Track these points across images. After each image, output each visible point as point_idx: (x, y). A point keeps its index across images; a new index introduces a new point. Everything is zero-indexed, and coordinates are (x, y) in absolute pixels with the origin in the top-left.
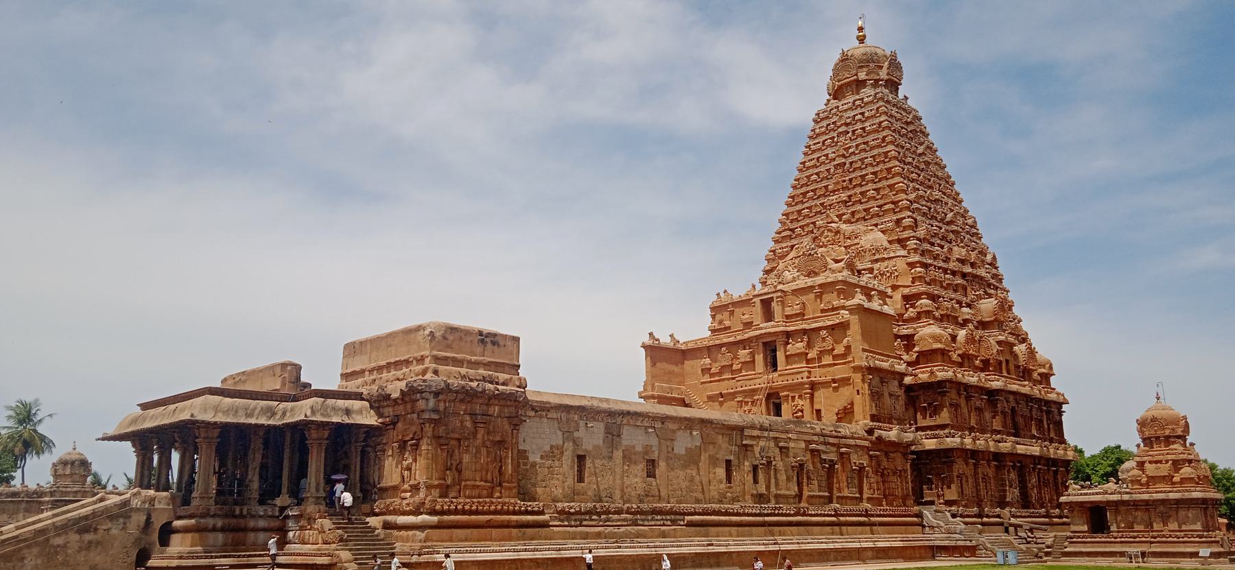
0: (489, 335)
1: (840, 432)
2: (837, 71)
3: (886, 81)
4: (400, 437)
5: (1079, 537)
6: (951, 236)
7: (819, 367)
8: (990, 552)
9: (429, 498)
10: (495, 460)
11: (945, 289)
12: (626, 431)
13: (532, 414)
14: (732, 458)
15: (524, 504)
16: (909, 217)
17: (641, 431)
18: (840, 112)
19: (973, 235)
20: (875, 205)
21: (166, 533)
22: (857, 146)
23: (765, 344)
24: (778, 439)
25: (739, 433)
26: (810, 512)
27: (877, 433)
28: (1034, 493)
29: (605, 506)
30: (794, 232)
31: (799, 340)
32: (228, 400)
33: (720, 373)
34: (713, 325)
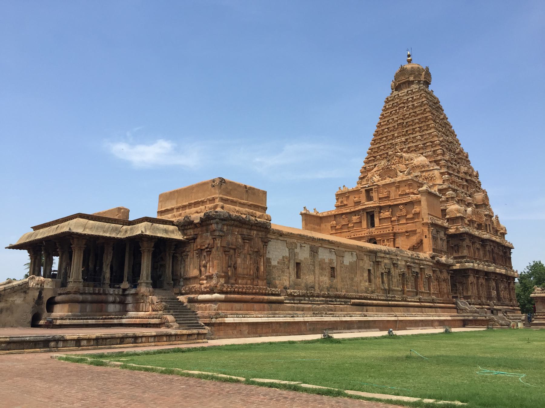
0: (251, 188)
1: (419, 257)
2: (397, 77)
3: (424, 81)
5: (541, 315)
6: (459, 161)
7: (398, 225)
8: (497, 323)
9: (219, 284)
10: (255, 263)
11: (459, 187)
12: (320, 250)
13: (273, 237)
14: (371, 268)
15: (270, 290)
16: (440, 149)
17: (328, 251)
18: (400, 97)
20: (421, 143)
21: (51, 304)
22: (410, 114)
23: (367, 213)
24: (393, 259)
25: (374, 255)
27: (436, 259)
28: (502, 293)
29: (312, 292)
32: (91, 222)
33: (341, 228)
34: (337, 203)
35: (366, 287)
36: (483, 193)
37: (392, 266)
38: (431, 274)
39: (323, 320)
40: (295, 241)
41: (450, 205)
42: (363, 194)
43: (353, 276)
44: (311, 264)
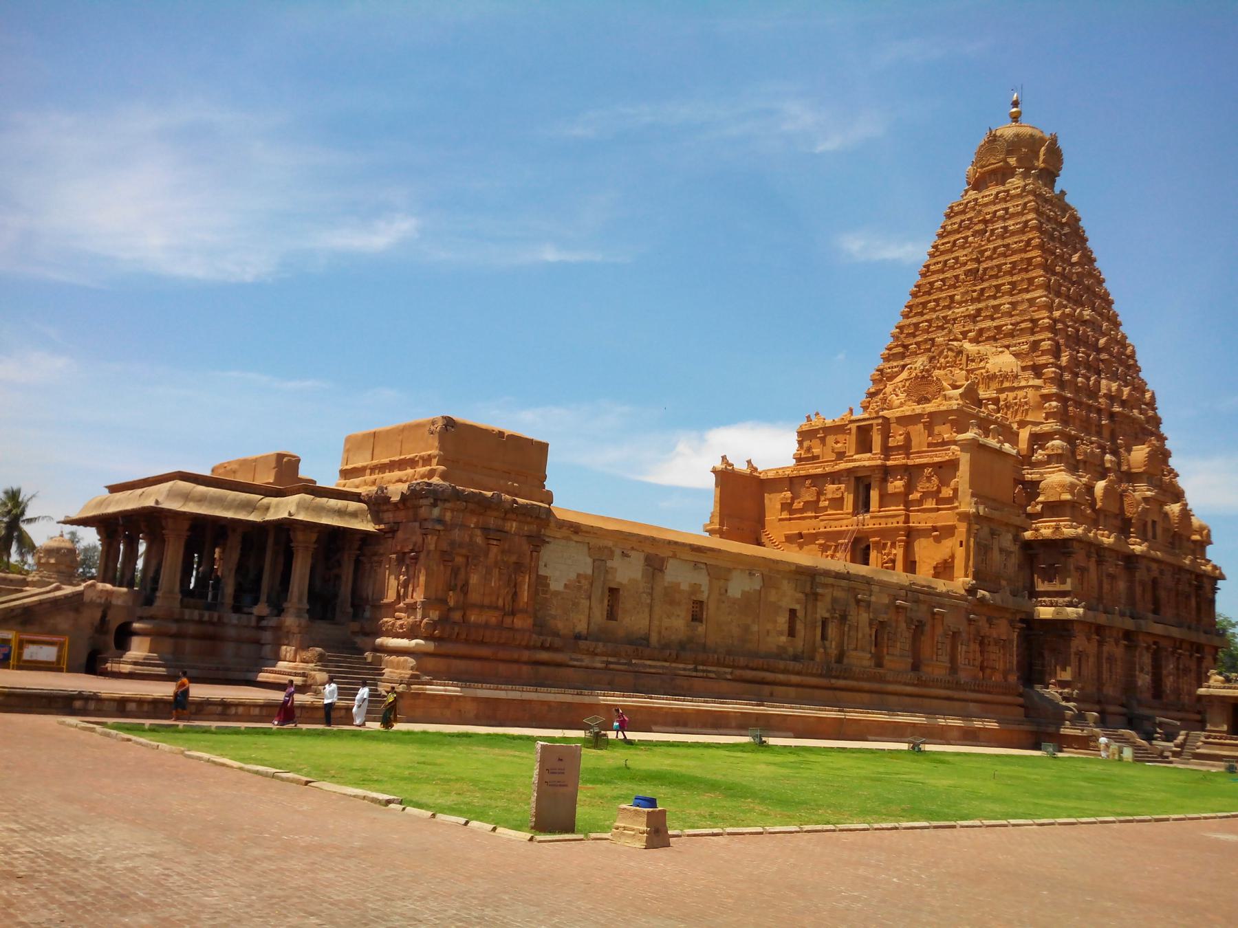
0: (513, 438)
1: (933, 588)
3: (1041, 170)
4: (399, 548)
7: (918, 511)
9: (425, 621)
14: (797, 607)
16: (1049, 339)
19: (1129, 367)
22: (995, 249)
23: (858, 479)
24: (857, 590)
27: (981, 593)
28: (1169, 682)
30: (908, 350)
31: (899, 477)
34: (799, 452)
35: (781, 644)
38: (963, 627)
40: (610, 544)
41: (1053, 472)
42: (852, 439)
44: (644, 592)
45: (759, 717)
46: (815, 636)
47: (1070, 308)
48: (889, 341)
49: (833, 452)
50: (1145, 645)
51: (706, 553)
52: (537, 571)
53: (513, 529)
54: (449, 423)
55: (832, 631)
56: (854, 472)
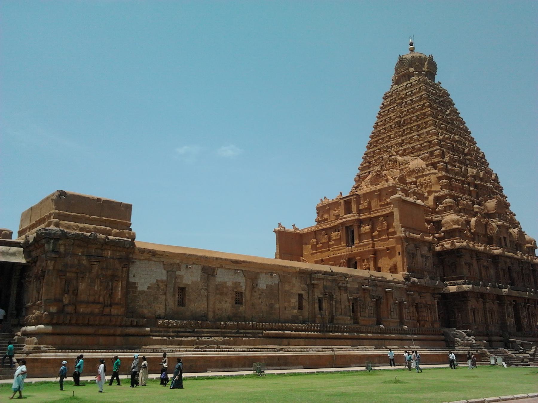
2: (396, 69)
3: (426, 72)
6: (468, 162)
7: (379, 240)
14: (303, 292)
19: (483, 163)
20: (418, 144)
23: (347, 228)
25: (308, 276)
26: (362, 330)
28: (525, 322)
35: (294, 314)
36: (496, 200)
37: (337, 289)
39: (318, 354)
40: (178, 262)
41: (448, 215)
42: (342, 208)
43: (273, 302)
44: (203, 289)
45: (279, 358)
46: (315, 308)
47: (448, 134)
48: (362, 161)
49: (334, 215)
50: (509, 302)
51: (241, 264)
52: (128, 280)
53: (109, 255)
54: (62, 193)
55: (325, 305)
56: (345, 224)
